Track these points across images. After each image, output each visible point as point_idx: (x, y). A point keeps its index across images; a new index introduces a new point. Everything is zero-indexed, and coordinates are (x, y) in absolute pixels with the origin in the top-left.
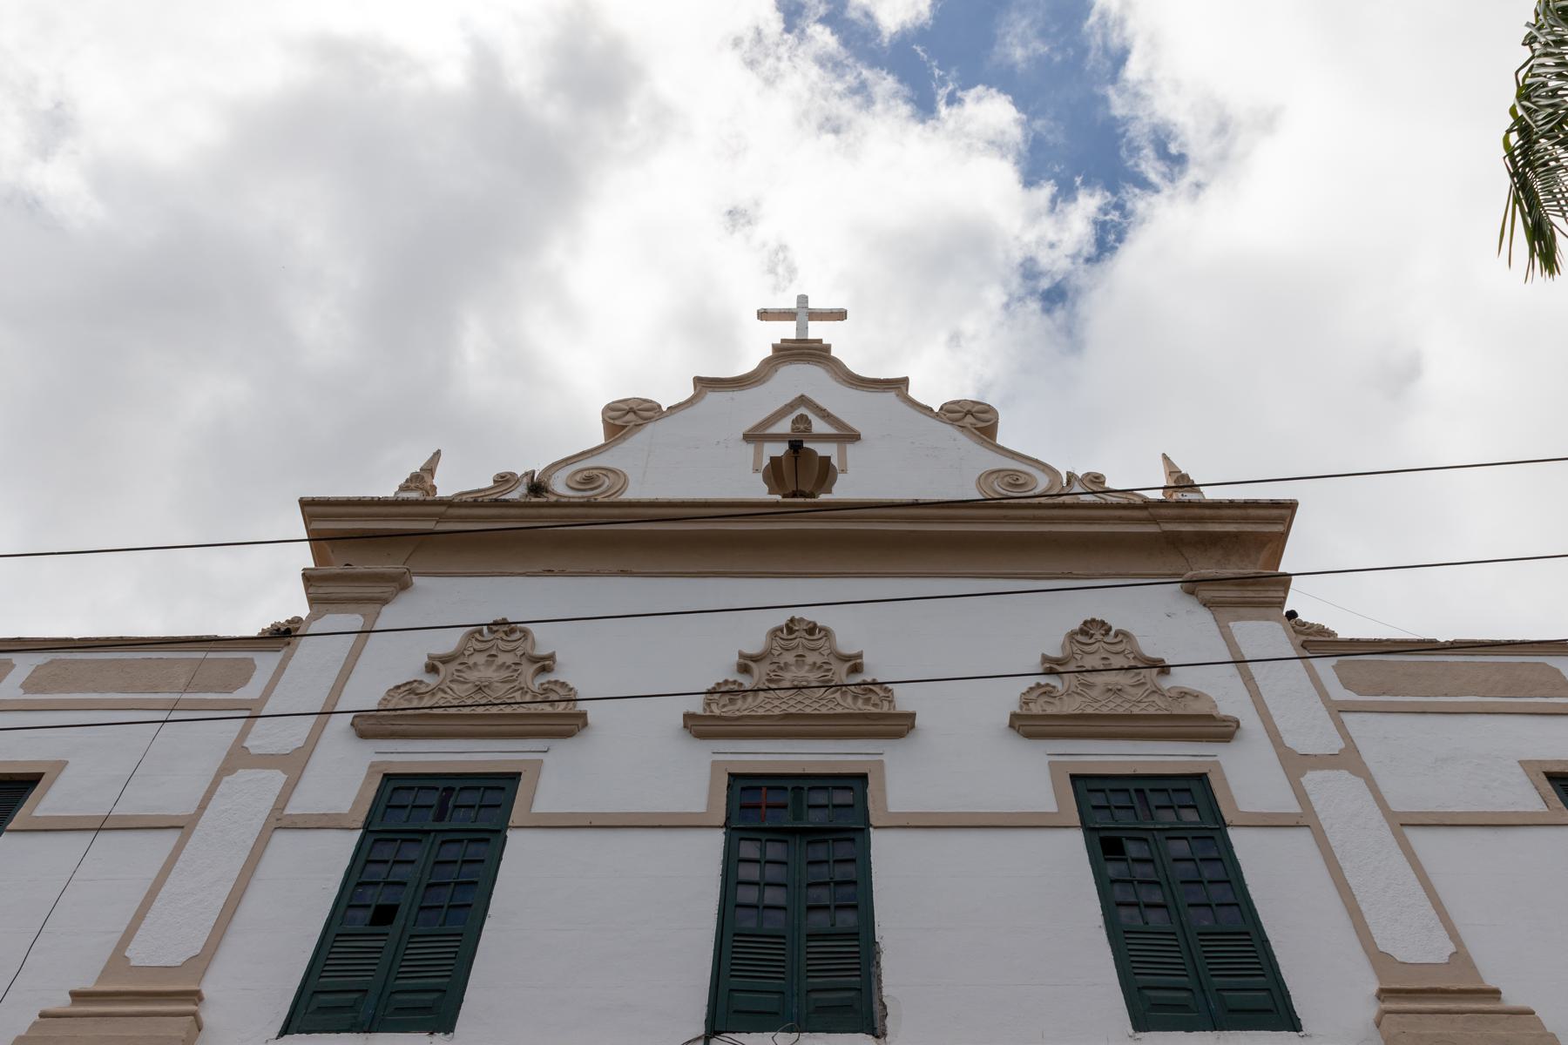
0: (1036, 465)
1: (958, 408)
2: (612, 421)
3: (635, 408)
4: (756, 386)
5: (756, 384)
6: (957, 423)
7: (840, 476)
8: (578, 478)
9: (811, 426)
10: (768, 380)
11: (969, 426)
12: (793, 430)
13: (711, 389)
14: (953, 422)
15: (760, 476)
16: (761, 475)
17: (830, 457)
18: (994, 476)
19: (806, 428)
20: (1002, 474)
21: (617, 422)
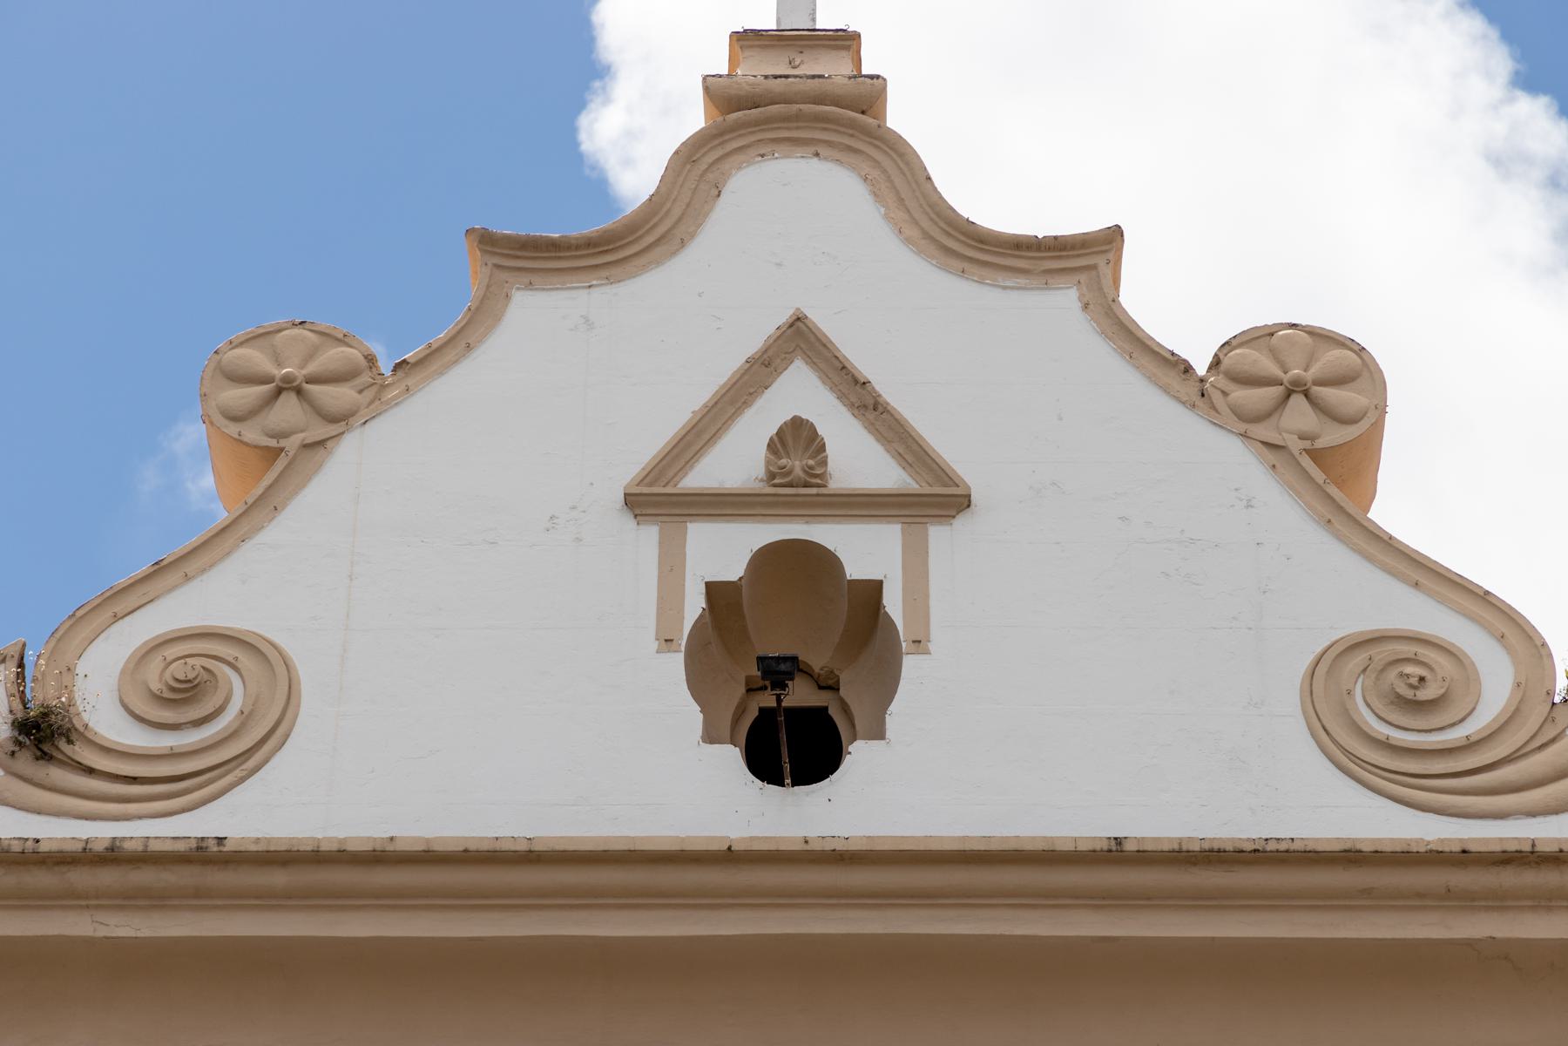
0: (1488, 615)
1: (1269, 367)
2: (232, 429)
3: (300, 374)
4: (658, 263)
5: (658, 250)
6: (1263, 431)
7: (911, 665)
8: (154, 676)
9: (824, 463)
10: (693, 236)
11: (1295, 445)
12: (771, 476)
13: (526, 278)
14: (1248, 418)
15: (676, 663)
16: (680, 657)
17: (881, 582)
18: (1360, 658)
19: (808, 471)
20: (1383, 653)
21: (252, 433)
